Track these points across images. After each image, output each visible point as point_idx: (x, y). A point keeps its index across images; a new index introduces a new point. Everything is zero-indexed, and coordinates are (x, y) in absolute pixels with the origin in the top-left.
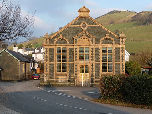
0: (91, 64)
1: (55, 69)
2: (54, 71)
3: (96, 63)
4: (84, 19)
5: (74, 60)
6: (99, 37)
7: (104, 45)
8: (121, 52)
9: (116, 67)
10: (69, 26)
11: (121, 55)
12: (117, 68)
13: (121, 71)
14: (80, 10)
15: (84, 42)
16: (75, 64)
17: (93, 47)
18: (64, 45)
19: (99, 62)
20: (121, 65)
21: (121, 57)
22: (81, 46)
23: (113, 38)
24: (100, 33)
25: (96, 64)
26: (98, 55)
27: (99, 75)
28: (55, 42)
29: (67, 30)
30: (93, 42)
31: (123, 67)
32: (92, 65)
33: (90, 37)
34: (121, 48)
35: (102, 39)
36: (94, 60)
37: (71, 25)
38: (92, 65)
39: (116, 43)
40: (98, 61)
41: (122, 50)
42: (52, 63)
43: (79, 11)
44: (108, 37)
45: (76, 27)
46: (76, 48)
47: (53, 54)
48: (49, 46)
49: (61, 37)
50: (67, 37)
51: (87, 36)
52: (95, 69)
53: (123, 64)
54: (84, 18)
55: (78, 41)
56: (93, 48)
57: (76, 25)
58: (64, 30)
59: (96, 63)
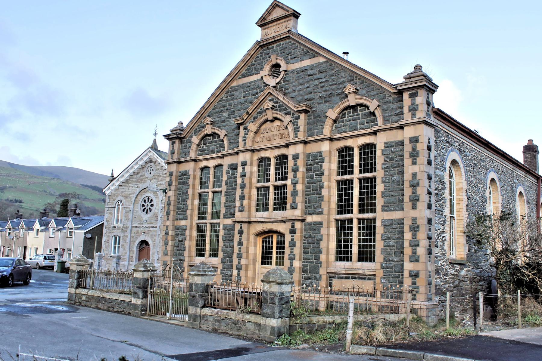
0: (288, 225)
1: (191, 244)
2: (186, 253)
3: (310, 219)
4: (277, 46)
5: (237, 209)
6: (324, 106)
7: (343, 138)
8: (407, 161)
9: (389, 238)
10: (234, 84)
11: (407, 177)
12: (392, 243)
13: (406, 258)
14: (263, 18)
15: (272, 133)
16: (237, 227)
17: (299, 149)
18: (216, 155)
19: (318, 214)
20: (406, 228)
21: (406, 185)
22: (263, 154)
23: (373, 99)
24: (326, 91)
25: (310, 224)
26: (318, 183)
27: (318, 277)
28: (194, 147)
29: (227, 101)
30: (297, 130)
31: (414, 237)
32: (293, 232)
33: (289, 110)
34: (406, 142)
35: (332, 114)
36: (300, 206)
37: (239, 79)
38: (293, 232)
39: (386, 120)
40: (318, 210)
41: (414, 149)
42: (183, 223)
43: (263, 23)
44: (352, 100)
45: (252, 82)
46: (244, 164)
47: (185, 191)
48: (181, 165)
49: (208, 130)
50: (227, 125)
51: (280, 111)
52: (305, 250)
53: (414, 220)
54: (275, 45)
55: (251, 135)
56: (298, 155)
57: (253, 74)
58: (220, 101)
59: (310, 219)
